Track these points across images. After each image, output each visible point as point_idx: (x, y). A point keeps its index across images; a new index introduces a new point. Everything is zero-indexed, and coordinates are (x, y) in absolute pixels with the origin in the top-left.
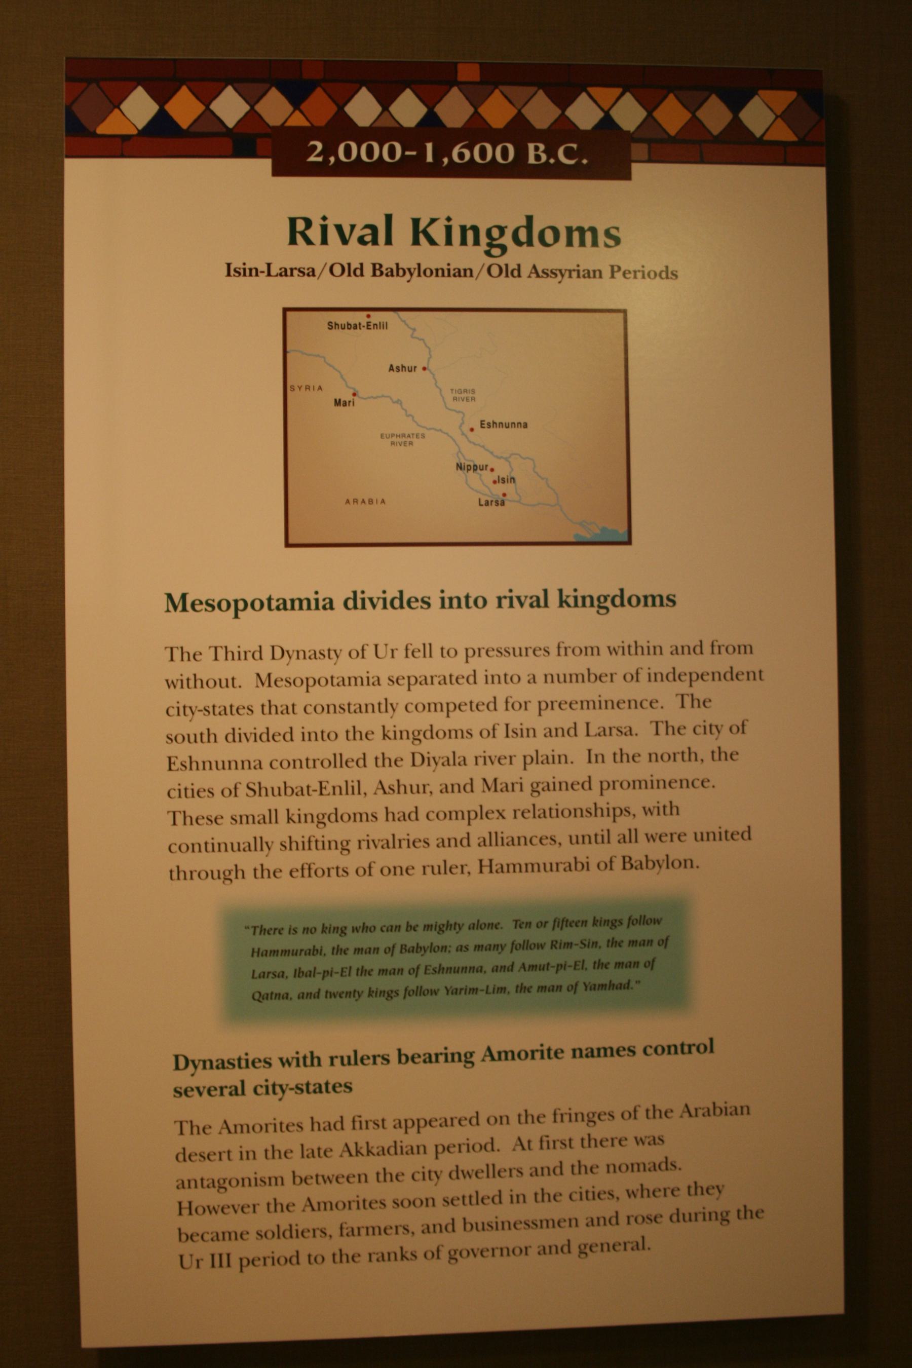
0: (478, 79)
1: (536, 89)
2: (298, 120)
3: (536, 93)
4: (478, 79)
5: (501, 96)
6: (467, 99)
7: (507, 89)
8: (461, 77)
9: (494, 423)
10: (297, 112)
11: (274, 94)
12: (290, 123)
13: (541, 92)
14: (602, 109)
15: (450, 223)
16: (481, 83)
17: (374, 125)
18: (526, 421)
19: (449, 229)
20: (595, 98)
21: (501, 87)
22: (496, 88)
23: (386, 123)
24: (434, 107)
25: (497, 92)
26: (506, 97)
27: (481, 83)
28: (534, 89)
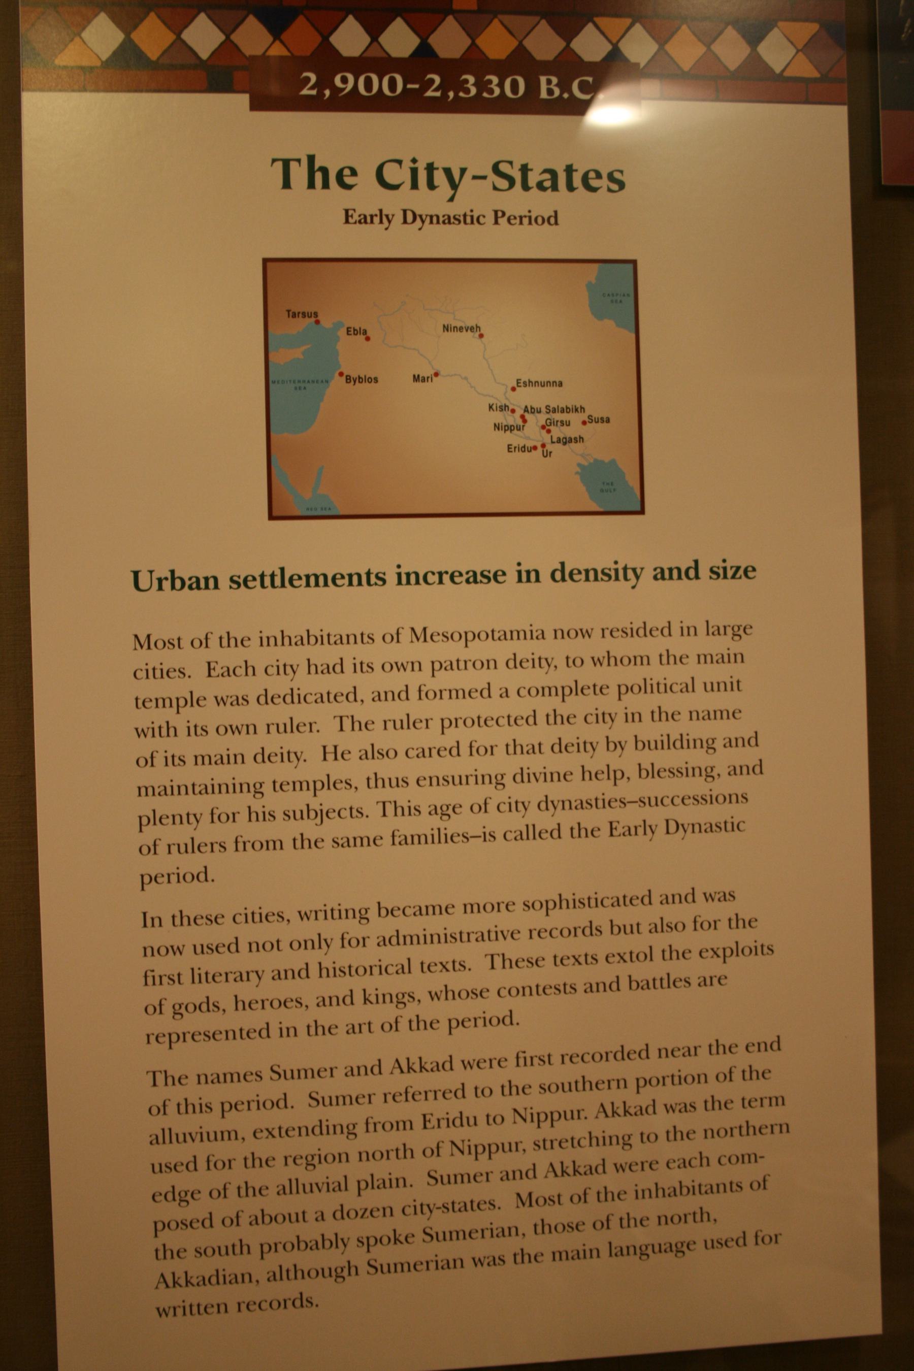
0: (475, 7)
1: (537, 18)
2: (278, 50)
3: (539, 22)
4: (475, 7)
5: (501, 26)
6: (464, 29)
7: (507, 19)
8: (456, 6)
9: (530, 382)
10: (277, 43)
11: (252, 21)
12: (272, 52)
13: (543, 22)
14: (610, 41)
15: (416, 165)
16: (480, 11)
17: (365, 55)
18: (561, 380)
19: (414, 172)
20: (602, 28)
21: (500, 17)
22: (495, 17)
23: (374, 53)
24: (428, 37)
25: (496, 21)
26: (506, 27)
27: (480, 11)
28: (533, 19)
